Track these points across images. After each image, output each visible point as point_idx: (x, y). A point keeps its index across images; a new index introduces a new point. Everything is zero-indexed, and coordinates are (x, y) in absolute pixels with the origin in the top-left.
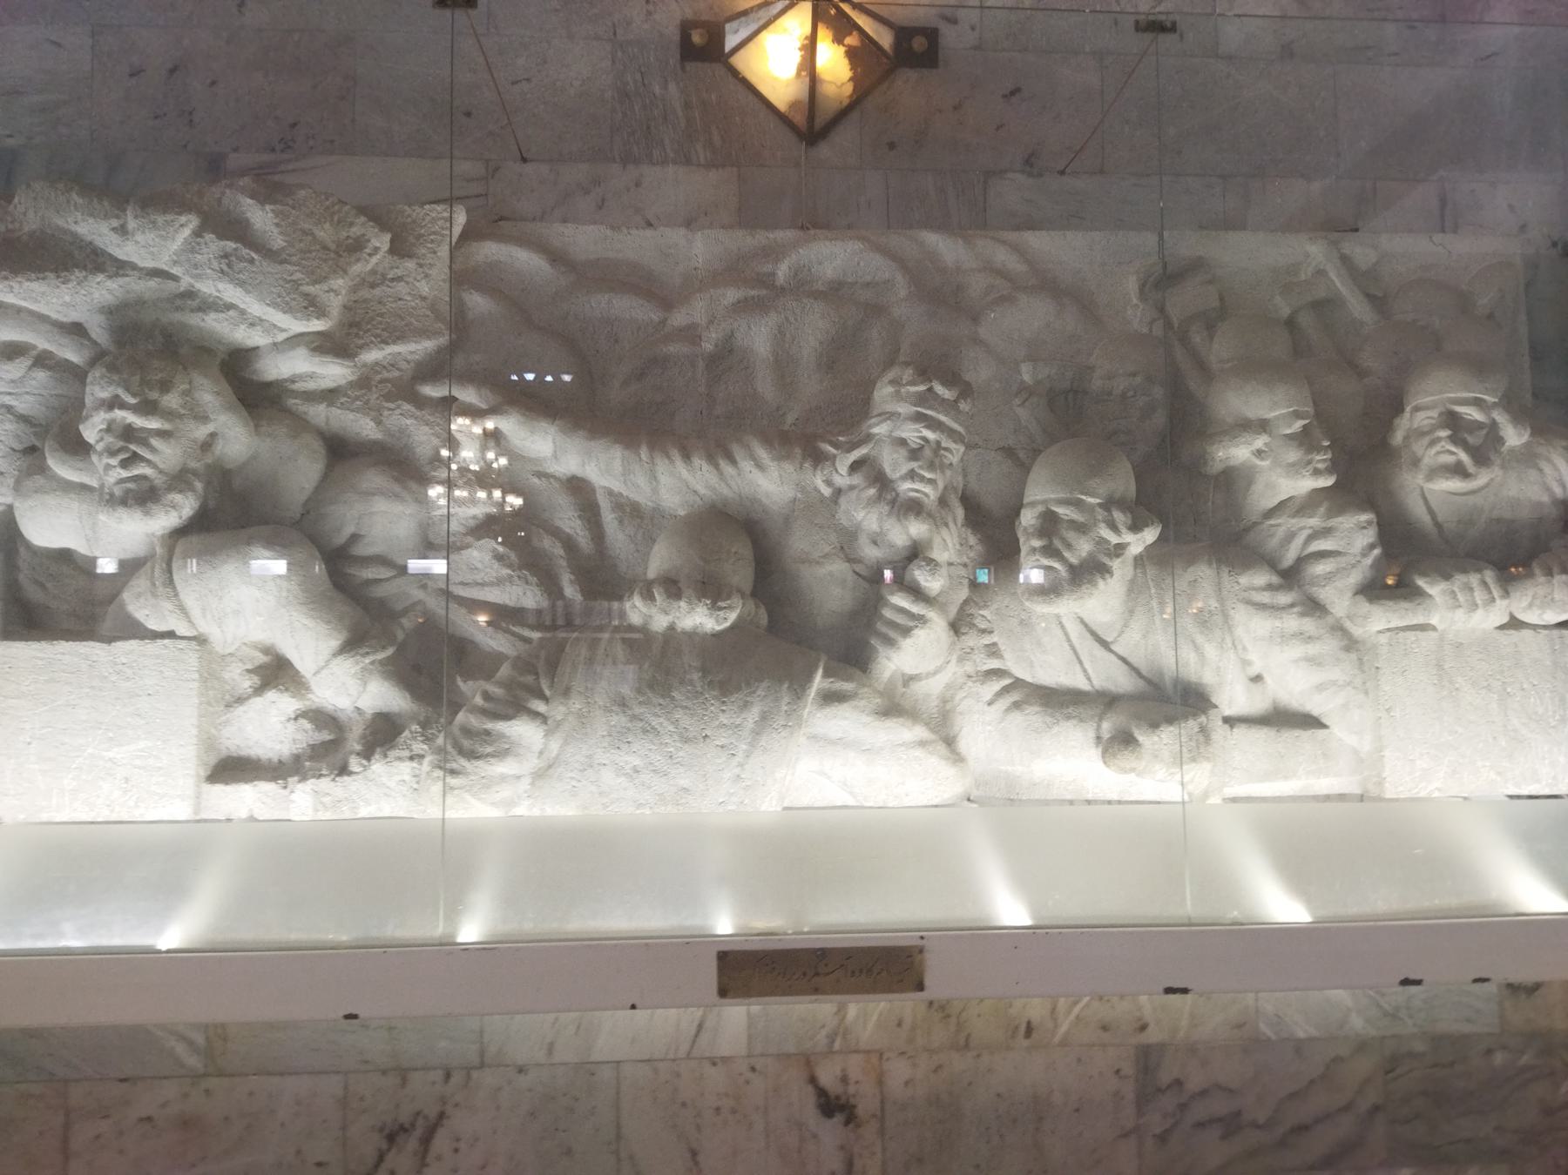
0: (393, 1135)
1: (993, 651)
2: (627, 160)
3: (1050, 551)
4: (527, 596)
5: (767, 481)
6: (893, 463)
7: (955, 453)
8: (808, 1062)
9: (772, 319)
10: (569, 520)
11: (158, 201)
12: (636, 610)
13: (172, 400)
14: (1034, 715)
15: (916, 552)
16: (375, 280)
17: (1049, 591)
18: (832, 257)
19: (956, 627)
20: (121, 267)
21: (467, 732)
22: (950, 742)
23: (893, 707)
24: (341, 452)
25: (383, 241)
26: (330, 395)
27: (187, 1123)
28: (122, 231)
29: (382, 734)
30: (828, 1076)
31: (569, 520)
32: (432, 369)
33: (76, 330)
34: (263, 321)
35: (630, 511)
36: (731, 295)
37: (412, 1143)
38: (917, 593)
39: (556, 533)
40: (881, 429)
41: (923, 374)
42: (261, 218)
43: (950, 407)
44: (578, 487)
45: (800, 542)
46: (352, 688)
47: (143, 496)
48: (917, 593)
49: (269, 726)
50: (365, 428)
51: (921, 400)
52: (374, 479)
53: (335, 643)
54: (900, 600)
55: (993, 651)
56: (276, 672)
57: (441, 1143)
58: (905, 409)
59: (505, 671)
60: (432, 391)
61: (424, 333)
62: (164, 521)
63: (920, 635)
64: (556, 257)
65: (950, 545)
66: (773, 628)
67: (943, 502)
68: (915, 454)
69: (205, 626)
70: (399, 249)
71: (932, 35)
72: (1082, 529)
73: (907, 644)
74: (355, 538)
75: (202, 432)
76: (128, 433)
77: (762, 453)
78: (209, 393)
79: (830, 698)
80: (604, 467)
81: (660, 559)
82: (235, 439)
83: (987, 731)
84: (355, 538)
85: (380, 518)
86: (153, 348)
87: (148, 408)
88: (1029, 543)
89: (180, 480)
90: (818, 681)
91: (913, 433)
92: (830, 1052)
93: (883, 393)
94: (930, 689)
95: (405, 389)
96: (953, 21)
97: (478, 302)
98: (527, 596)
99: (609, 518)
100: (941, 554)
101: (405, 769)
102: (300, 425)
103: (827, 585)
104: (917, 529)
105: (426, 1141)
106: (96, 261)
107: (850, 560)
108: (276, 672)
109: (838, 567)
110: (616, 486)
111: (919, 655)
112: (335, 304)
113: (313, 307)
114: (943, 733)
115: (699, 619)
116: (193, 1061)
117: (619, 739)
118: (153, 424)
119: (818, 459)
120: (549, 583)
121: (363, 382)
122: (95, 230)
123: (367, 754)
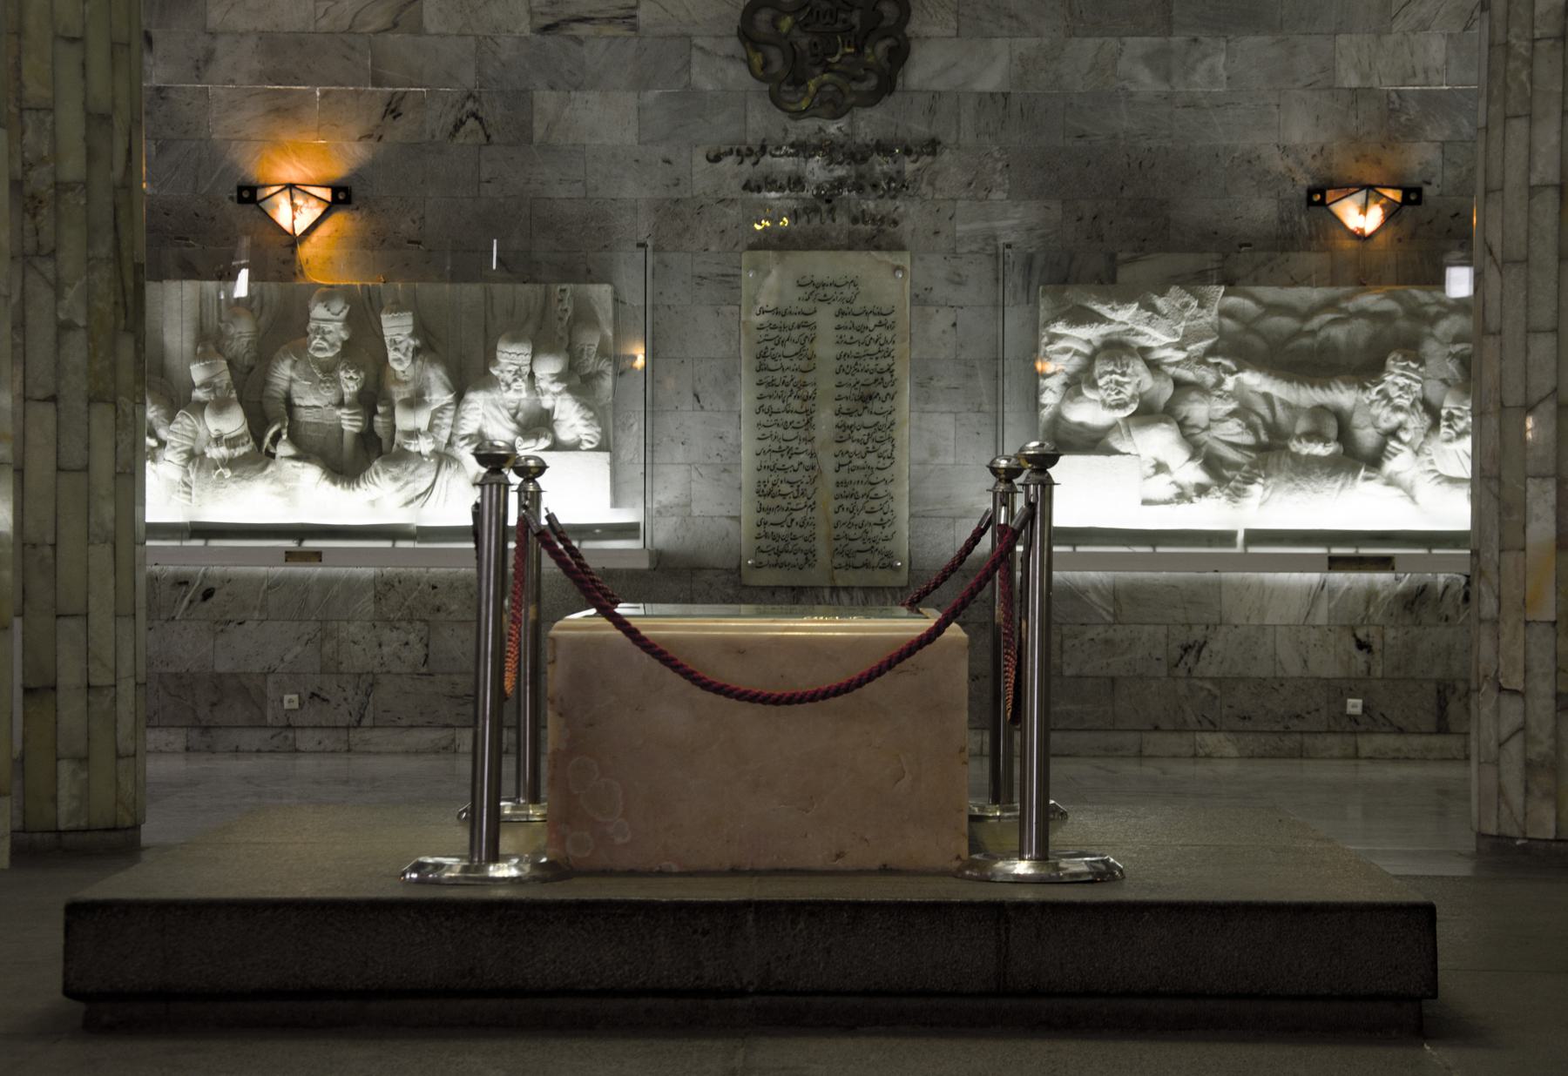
0: (1186, 649)
1: (1431, 462)
2: (1284, 250)
3: (1450, 426)
4: (1248, 439)
5: (1343, 397)
6: (1394, 392)
7: (1417, 387)
8: (1353, 630)
9: (1347, 327)
10: (1263, 409)
11: (1125, 300)
12: (1295, 446)
13: (1129, 371)
14: (1446, 487)
15: (1401, 426)
16: (1194, 318)
17: (1449, 441)
18: (1371, 300)
19: (1417, 453)
20: (1111, 321)
21: (1237, 489)
22: (1413, 498)
23: (1391, 482)
24: (1179, 384)
25: (1195, 303)
26: (1177, 364)
27: (1107, 642)
28: (1113, 309)
29: (1202, 490)
30: (1361, 634)
31: (1263, 409)
32: (1211, 351)
33: (1089, 342)
34: (1157, 337)
35: (1287, 405)
36: (1329, 317)
37: (1194, 652)
38: (1400, 441)
39: (1258, 415)
40: (1389, 378)
41: (1405, 358)
42: (1160, 303)
43: (1415, 371)
44: (1267, 397)
45: (1357, 420)
46: (1193, 474)
47: (1121, 405)
48: (1400, 441)
49: (1161, 487)
50: (1188, 375)
51: (1404, 368)
52: (1194, 396)
53: (1187, 457)
54: (1393, 443)
55: (1431, 462)
56: (1160, 467)
57: (1205, 652)
58: (1398, 371)
59: (1246, 468)
60: (1212, 360)
61: (1209, 337)
62: (1121, 414)
63: (1400, 456)
64: (1258, 301)
65: (1416, 423)
66: (1345, 453)
67: (1413, 405)
68: (1401, 389)
69: (1140, 451)
70: (1201, 306)
71: (1418, 191)
72: (1461, 418)
73: (1395, 459)
74: (1186, 418)
75: (1136, 380)
76: (1118, 383)
77: (1342, 387)
78: (1138, 366)
79: (1366, 479)
80: (1279, 390)
81: (1302, 425)
82: (1148, 382)
83: (1427, 490)
84: (1186, 418)
85: (1198, 411)
86: (1116, 349)
87: (1123, 374)
88: (1443, 423)
89: (1133, 397)
90: (1362, 473)
91: (1402, 381)
92: (1362, 624)
93: (1390, 362)
94: (1406, 477)
95: (1202, 361)
96: (1429, 183)
97: (1227, 322)
98: (1248, 439)
99: (1279, 409)
100: (1410, 425)
101: (1214, 501)
102: (1167, 376)
103: (1367, 437)
104: (1401, 417)
105: (1199, 651)
106: (1100, 319)
107: (1376, 427)
108: (1160, 467)
109: (1371, 431)
110: (1284, 397)
111: (1400, 463)
112: (1181, 331)
113: (1176, 333)
114: (1410, 493)
115: (1319, 450)
116: (1109, 619)
117: (1291, 491)
118: (1125, 379)
119: (1365, 389)
120: (1256, 433)
121: (1188, 359)
122: (1104, 310)
123: (1199, 496)
